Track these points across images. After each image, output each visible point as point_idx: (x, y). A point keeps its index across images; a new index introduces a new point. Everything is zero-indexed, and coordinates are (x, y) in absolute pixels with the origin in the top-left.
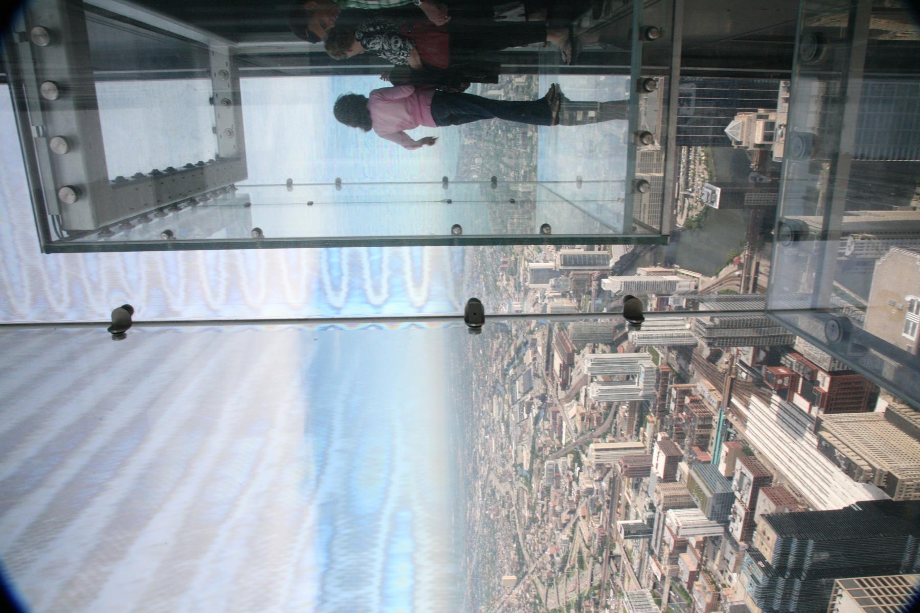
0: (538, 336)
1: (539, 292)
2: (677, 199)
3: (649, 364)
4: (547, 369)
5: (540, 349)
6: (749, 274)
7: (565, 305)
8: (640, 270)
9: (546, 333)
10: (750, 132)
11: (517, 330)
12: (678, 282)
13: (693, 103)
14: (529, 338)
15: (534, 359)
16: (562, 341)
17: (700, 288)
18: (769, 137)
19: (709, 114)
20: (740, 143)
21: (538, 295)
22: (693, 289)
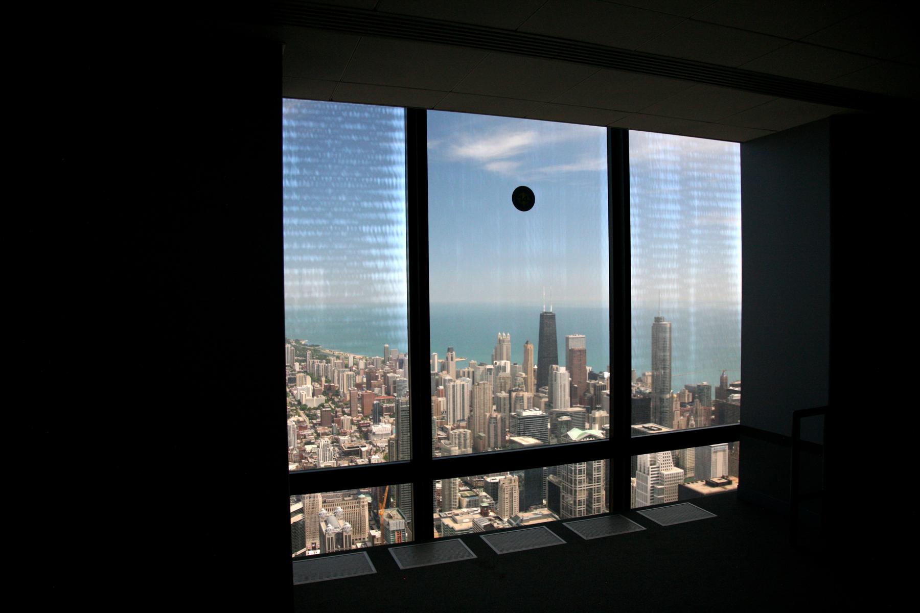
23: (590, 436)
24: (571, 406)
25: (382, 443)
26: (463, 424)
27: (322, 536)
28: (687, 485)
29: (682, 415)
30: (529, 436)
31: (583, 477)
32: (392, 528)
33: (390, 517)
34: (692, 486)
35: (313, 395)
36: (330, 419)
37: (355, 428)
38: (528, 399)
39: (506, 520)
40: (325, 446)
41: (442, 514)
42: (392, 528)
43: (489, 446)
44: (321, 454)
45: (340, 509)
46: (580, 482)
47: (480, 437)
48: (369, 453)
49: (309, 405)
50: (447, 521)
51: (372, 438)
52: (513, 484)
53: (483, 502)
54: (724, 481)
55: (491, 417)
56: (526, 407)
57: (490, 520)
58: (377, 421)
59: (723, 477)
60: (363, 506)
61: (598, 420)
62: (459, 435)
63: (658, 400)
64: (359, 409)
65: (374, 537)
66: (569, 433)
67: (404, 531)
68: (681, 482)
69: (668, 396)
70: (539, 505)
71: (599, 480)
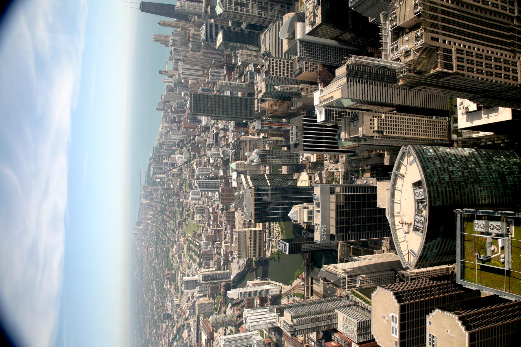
0: (191, 321)
1: (190, 293)
2: (266, 242)
3: (259, 338)
4: (197, 342)
5: (192, 329)
6: (308, 284)
7: (206, 302)
8: (249, 283)
9: (196, 319)
10: (301, 215)
11: (177, 318)
12: (270, 289)
13: (270, 195)
14: (186, 322)
15: (189, 336)
16: (206, 323)
17: (283, 292)
18: (310, 218)
19: (279, 205)
20: (297, 221)
21: (190, 295)
22: (279, 293)
24: (202, 2)
25: (213, 121)
26: (206, 71)
27: (259, 165)
31: (245, 9)
32: (260, 128)
33: (254, 128)
35: (182, 154)
36: (196, 148)
37: (202, 134)
39: (264, 61)
40: (211, 153)
41: (256, 97)
42: (260, 128)
43: (221, 59)
44: (216, 156)
45: (246, 154)
46: (248, 12)
47: (215, 63)
48: (217, 128)
49: (188, 157)
50: (260, 96)
51: (208, 126)
52: (244, 53)
55: (203, 56)
56: (199, 33)
57: (263, 72)
58: (200, 121)
60: (246, 138)
62: (212, 76)
64: (192, 130)
65: (263, 137)
67: (262, 121)
70: (258, 36)
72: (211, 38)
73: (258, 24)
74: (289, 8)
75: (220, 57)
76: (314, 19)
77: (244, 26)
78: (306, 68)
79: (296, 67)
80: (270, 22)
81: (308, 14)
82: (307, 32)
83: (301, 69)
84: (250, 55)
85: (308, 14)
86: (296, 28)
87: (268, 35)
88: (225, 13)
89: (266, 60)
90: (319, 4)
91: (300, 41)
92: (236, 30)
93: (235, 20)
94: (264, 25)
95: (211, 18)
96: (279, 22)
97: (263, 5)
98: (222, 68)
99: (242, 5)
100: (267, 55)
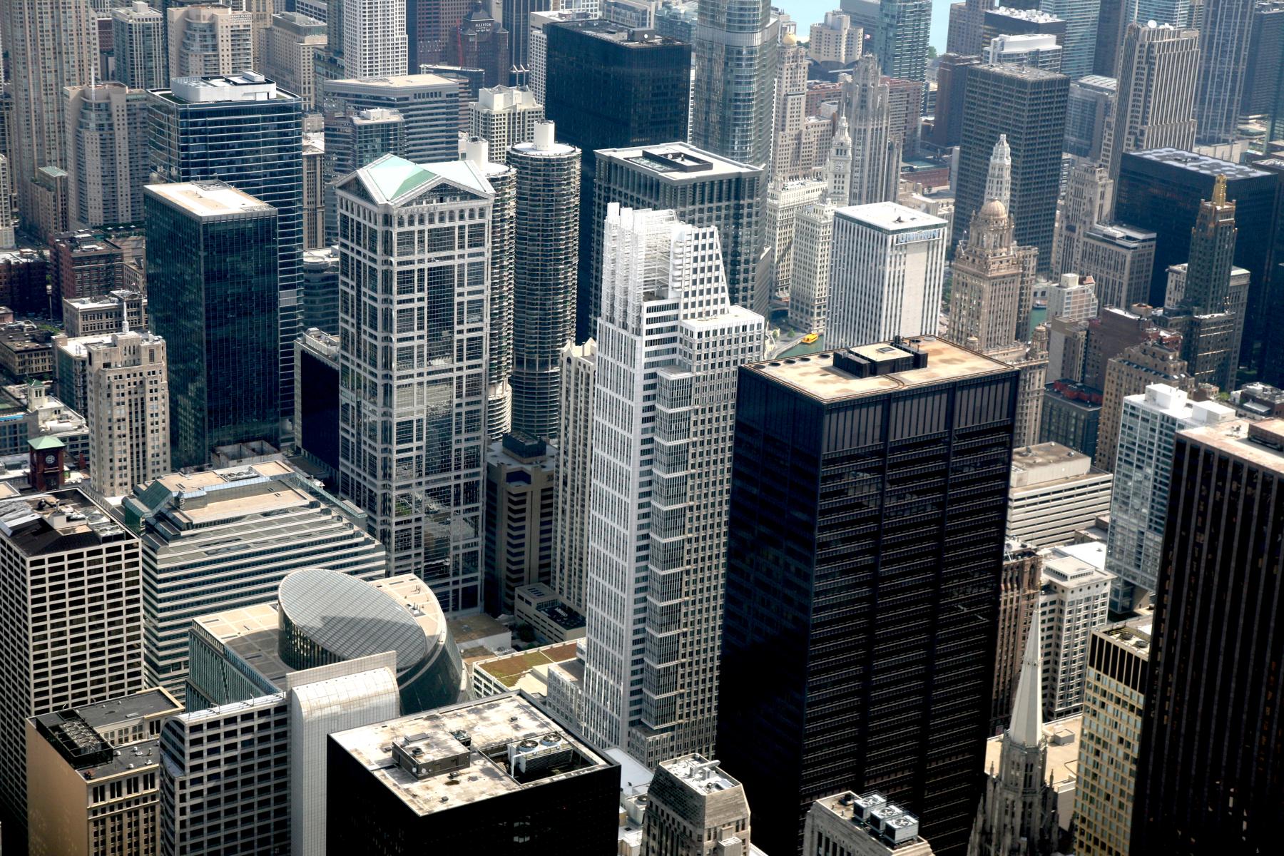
23: (444, 191)
24: (414, 70)
28: (770, 371)
29: (812, 109)
30: (227, 180)
31: (418, 339)
34: (787, 375)
38: (236, 35)
39: (115, 501)
43: (83, 219)
46: (406, 356)
47: (46, 182)
52: (146, 366)
53: (40, 434)
54: (899, 354)
55: (85, 104)
56: (226, 69)
57: (40, 506)
59: (897, 342)
61: (501, 129)
63: (719, 55)
66: (362, 173)
68: (750, 360)
69: (758, 39)
70: (274, 442)
71: (474, 348)
72: (212, 143)
73: (346, 431)
74: (468, 598)
75: (96, 214)
76: (435, 768)
77: (319, 343)
78: (116, 787)
79: (112, 716)
80: (367, 501)
81: (453, 724)
82: (347, 740)
83: (105, 754)
84: (139, 408)
85: (453, 719)
86: (362, 668)
87: (289, 499)
88: (371, 216)
89: (129, 516)
90: (521, 777)
91: (281, 709)
92: (287, 298)
93: (347, 286)
94: (346, 466)
95: (331, 134)
96: (377, 555)
97: (460, 442)
98: (27, 233)
99: (440, 314)
100: (161, 517)
